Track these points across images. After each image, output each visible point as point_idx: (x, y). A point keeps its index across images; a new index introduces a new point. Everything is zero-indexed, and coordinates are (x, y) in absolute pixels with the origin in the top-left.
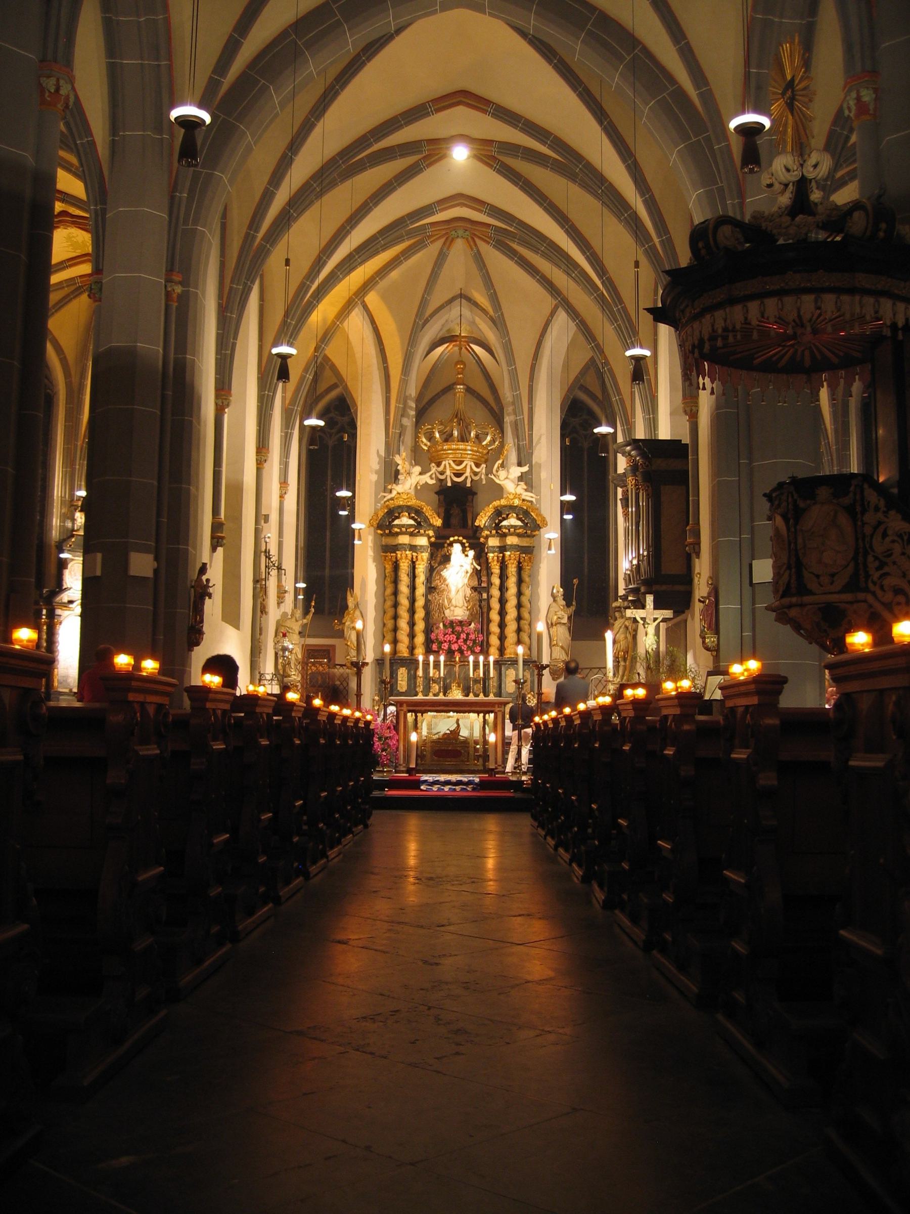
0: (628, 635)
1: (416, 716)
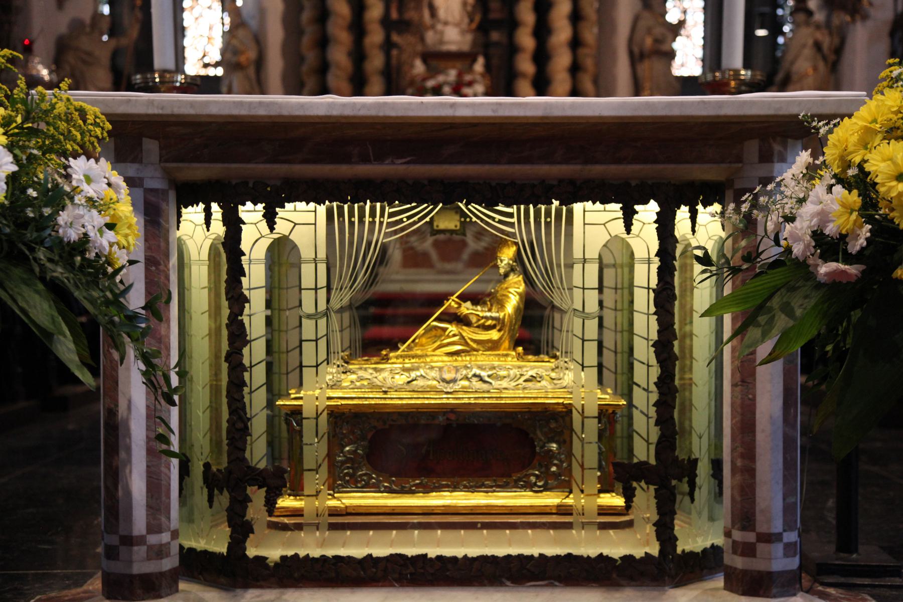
0: (821, 65)
1: (233, 224)
